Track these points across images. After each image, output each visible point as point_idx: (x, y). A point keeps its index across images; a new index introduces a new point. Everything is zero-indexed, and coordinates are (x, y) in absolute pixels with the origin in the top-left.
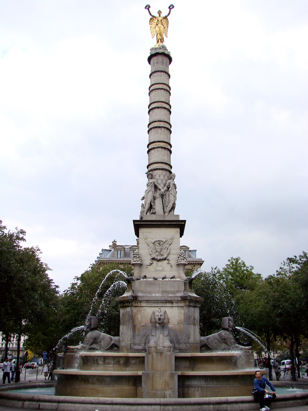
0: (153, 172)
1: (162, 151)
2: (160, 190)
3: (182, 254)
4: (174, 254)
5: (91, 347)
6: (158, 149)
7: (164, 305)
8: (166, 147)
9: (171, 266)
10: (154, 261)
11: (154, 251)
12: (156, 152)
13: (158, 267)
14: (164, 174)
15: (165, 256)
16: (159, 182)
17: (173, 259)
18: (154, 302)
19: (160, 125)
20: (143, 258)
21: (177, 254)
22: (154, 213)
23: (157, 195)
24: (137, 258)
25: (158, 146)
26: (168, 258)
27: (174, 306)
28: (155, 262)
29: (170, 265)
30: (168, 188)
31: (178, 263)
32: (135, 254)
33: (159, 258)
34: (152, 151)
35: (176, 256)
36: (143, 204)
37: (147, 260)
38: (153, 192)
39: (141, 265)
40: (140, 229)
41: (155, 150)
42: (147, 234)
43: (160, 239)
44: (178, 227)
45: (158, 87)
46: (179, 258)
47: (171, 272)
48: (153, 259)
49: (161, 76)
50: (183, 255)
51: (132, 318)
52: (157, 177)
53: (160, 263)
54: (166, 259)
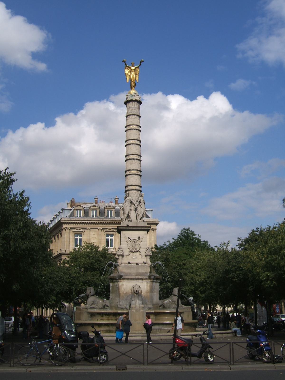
0: (129, 191)
1: (136, 176)
2: (134, 205)
5: (91, 306)
6: (133, 175)
7: (138, 281)
9: (142, 256)
10: (131, 253)
11: (131, 246)
12: (131, 177)
13: (133, 257)
14: (137, 193)
15: (138, 250)
16: (134, 199)
17: (143, 251)
18: (132, 279)
19: (134, 158)
21: (145, 248)
22: (131, 221)
23: (133, 208)
25: (132, 173)
26: (139, 251)
27: (144, 281)
28: (131, 253)
30: (140, 203)
31: (146, 254)
33: (134, 250)
34: (128, 177)
35: (145, 250)
37: (126, 252)
38: (129, 206)
39: (123, 256)
40: (122, 232)
41: (131, 175)
42: (126, 235)
43: (135, 239)
45: (132, 128)
46: (147, 251)
47: (142, 260)
48: (131, 251)
49: (134, 119)
50: (149, 249)
51: (118, 289)
52: (132, 195)
53: (135, 254)
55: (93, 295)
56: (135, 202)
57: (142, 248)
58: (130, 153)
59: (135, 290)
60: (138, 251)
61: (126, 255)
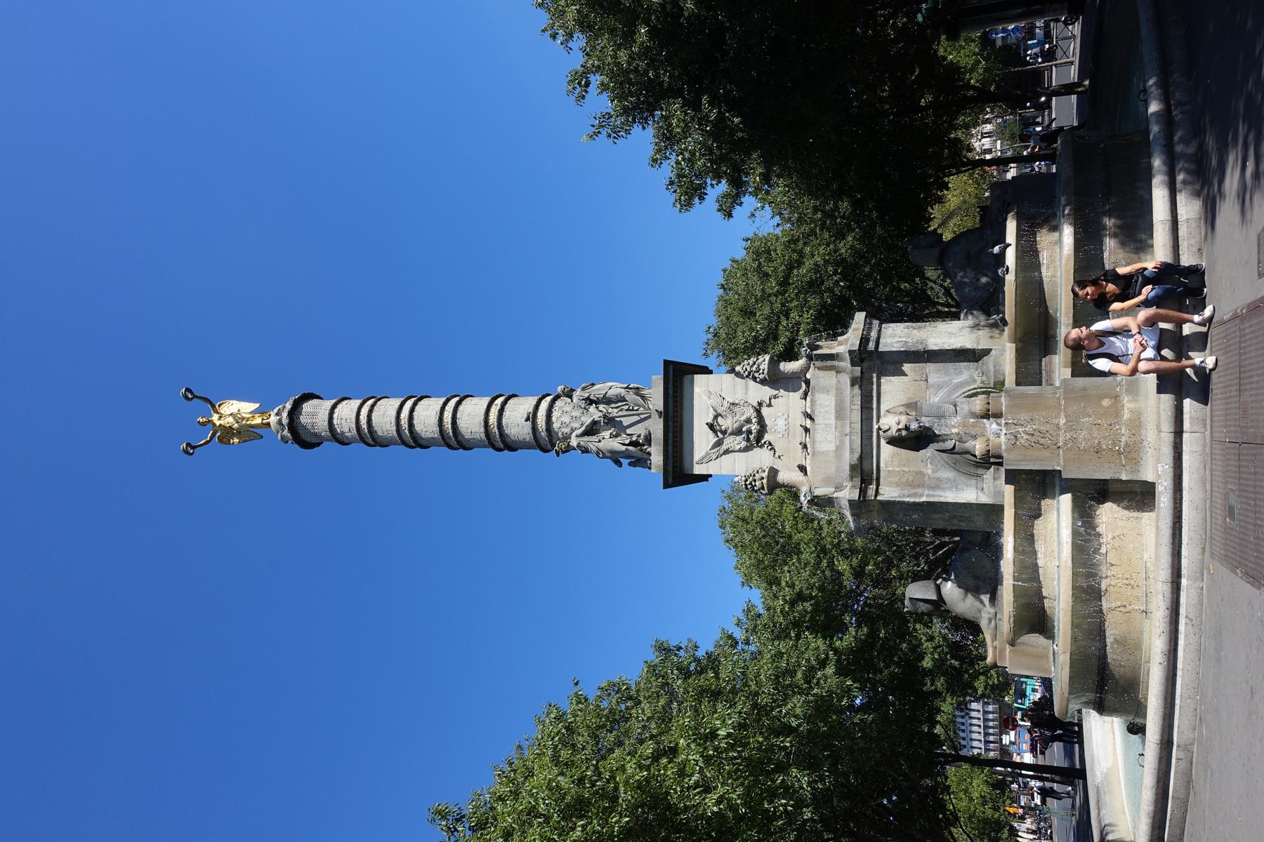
3: (746, 370)
8: (499, 407)
9: (775, 397)
15: (750, 413)
20: (757, 466)
24: (755, 481)
28: (767, 437)
29: (773, 400)
32: (746, 485)
33: (754, 427)
36: (630, 464)
44: (682, 379)
46: (757, 375)
54: (757, 409)
55: (938, 589)
56: (588, 420)
57: (746, 393)
59: (904, 433)
61: (771, 457)
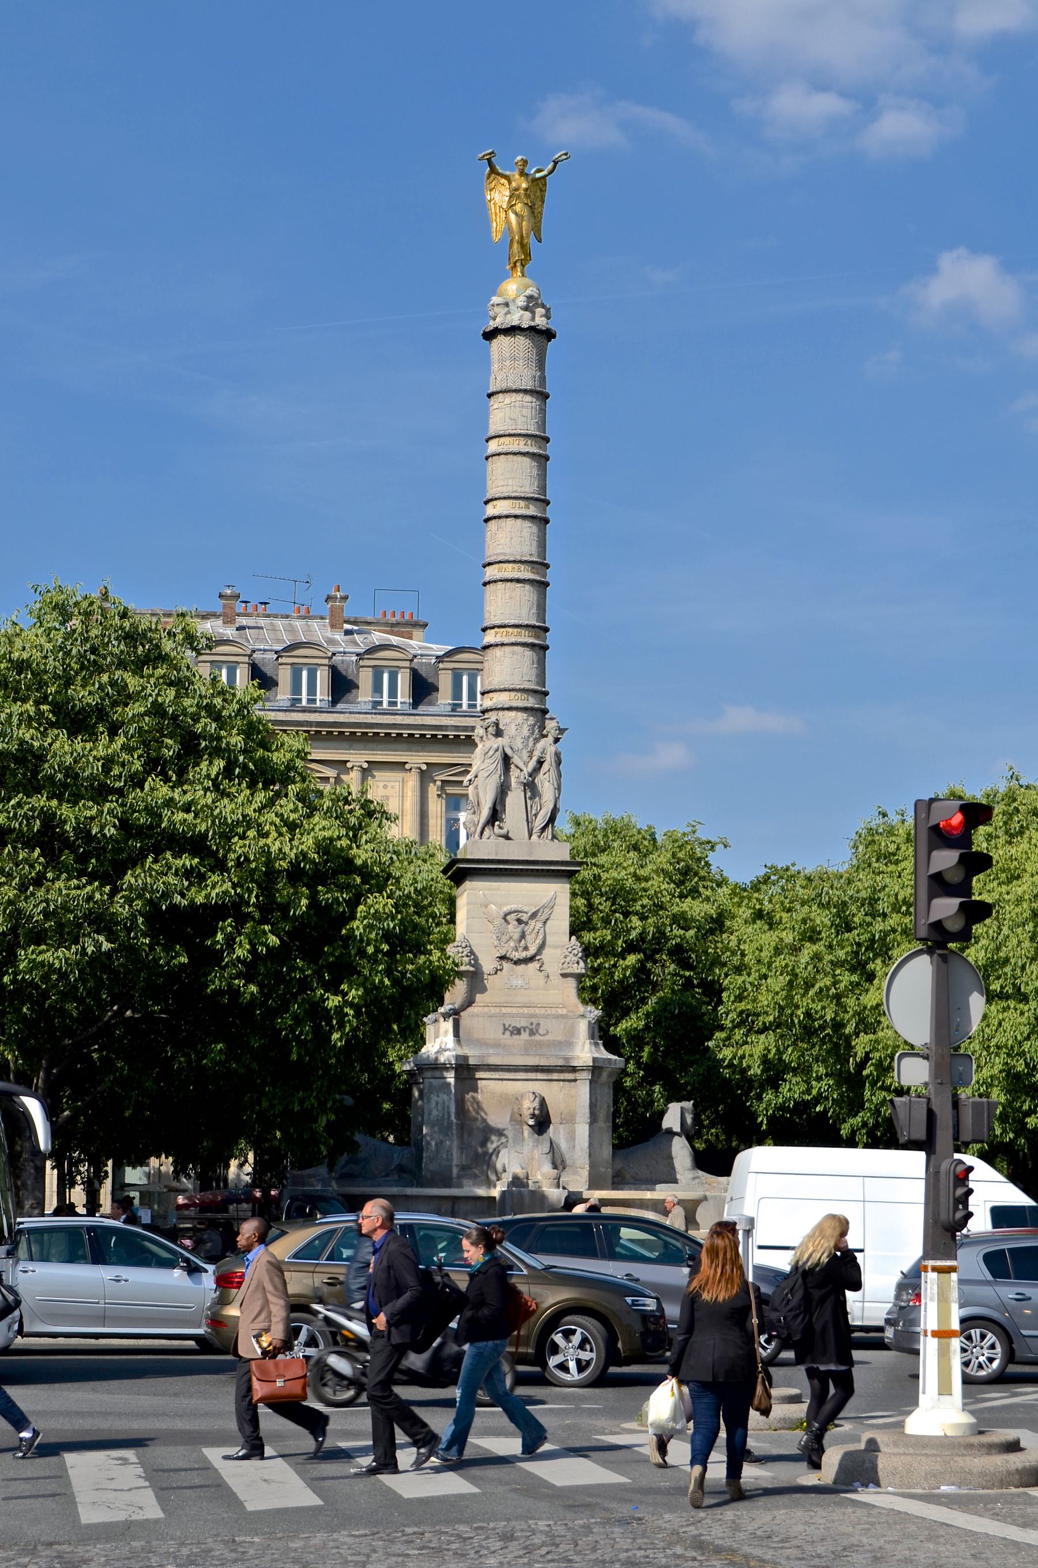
4: (556, 947)
28: (506, 965)
30: (540, 763)
33: (516, 955)
37: (488, 964)
42: (486, 892)
43: (519, 907)
46: (568, 959)
58: (505, 554)
60: (531, 959)
